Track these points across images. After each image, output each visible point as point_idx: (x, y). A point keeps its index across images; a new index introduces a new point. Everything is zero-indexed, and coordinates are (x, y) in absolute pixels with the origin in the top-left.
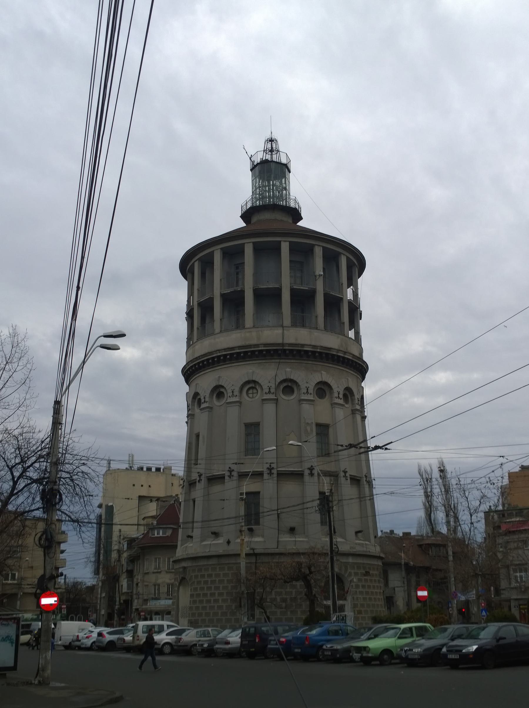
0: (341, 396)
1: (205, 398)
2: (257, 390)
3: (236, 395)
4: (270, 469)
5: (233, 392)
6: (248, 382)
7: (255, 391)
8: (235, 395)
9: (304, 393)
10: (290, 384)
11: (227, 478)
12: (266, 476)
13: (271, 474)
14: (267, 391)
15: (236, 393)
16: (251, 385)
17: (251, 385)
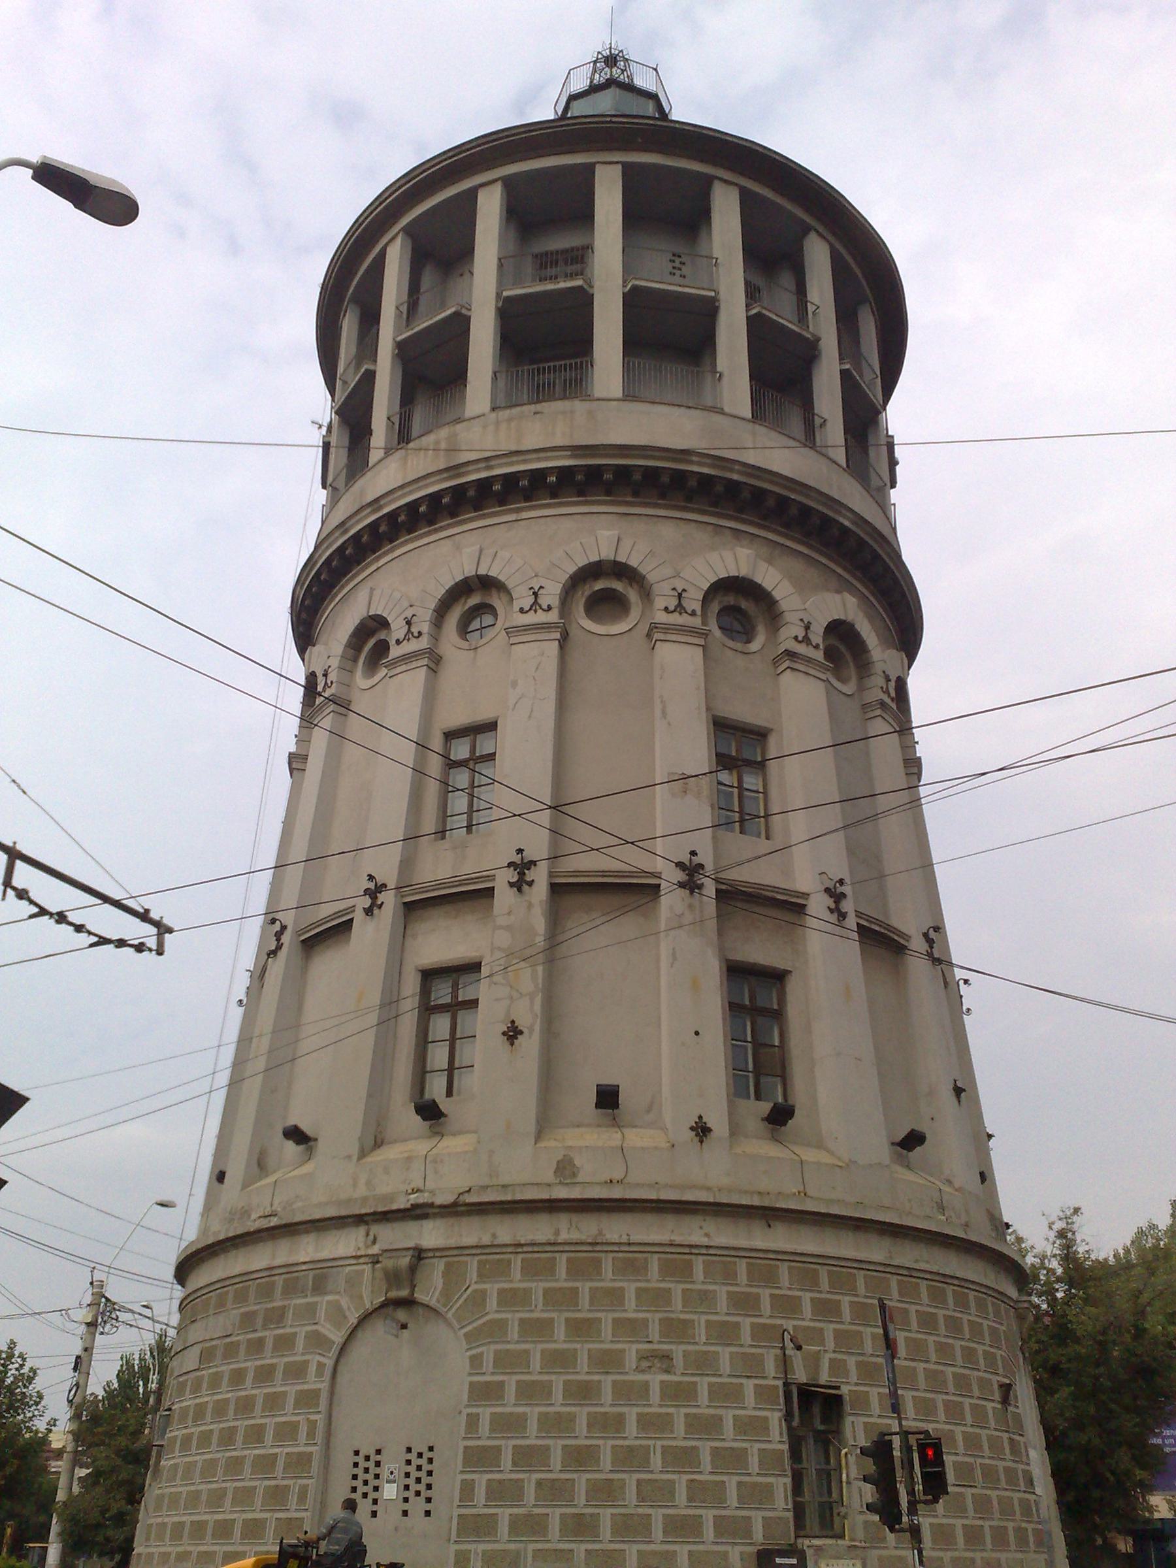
0: (817, 636)
1: (325, 675)
2: (495, 615)
3: (420, 633)
4: (522, 866)
5: (409, 623)
6: (462, 589)
7: (488, 619)
8: (416, 634)
9: (666, 609)
10: (618, 586)
11: (359, 916)
12: (504, 897)
13: (519, 885)
14: (527, 602)
15: (423, 625)
16: (474, 600)
17: (474, 600)
